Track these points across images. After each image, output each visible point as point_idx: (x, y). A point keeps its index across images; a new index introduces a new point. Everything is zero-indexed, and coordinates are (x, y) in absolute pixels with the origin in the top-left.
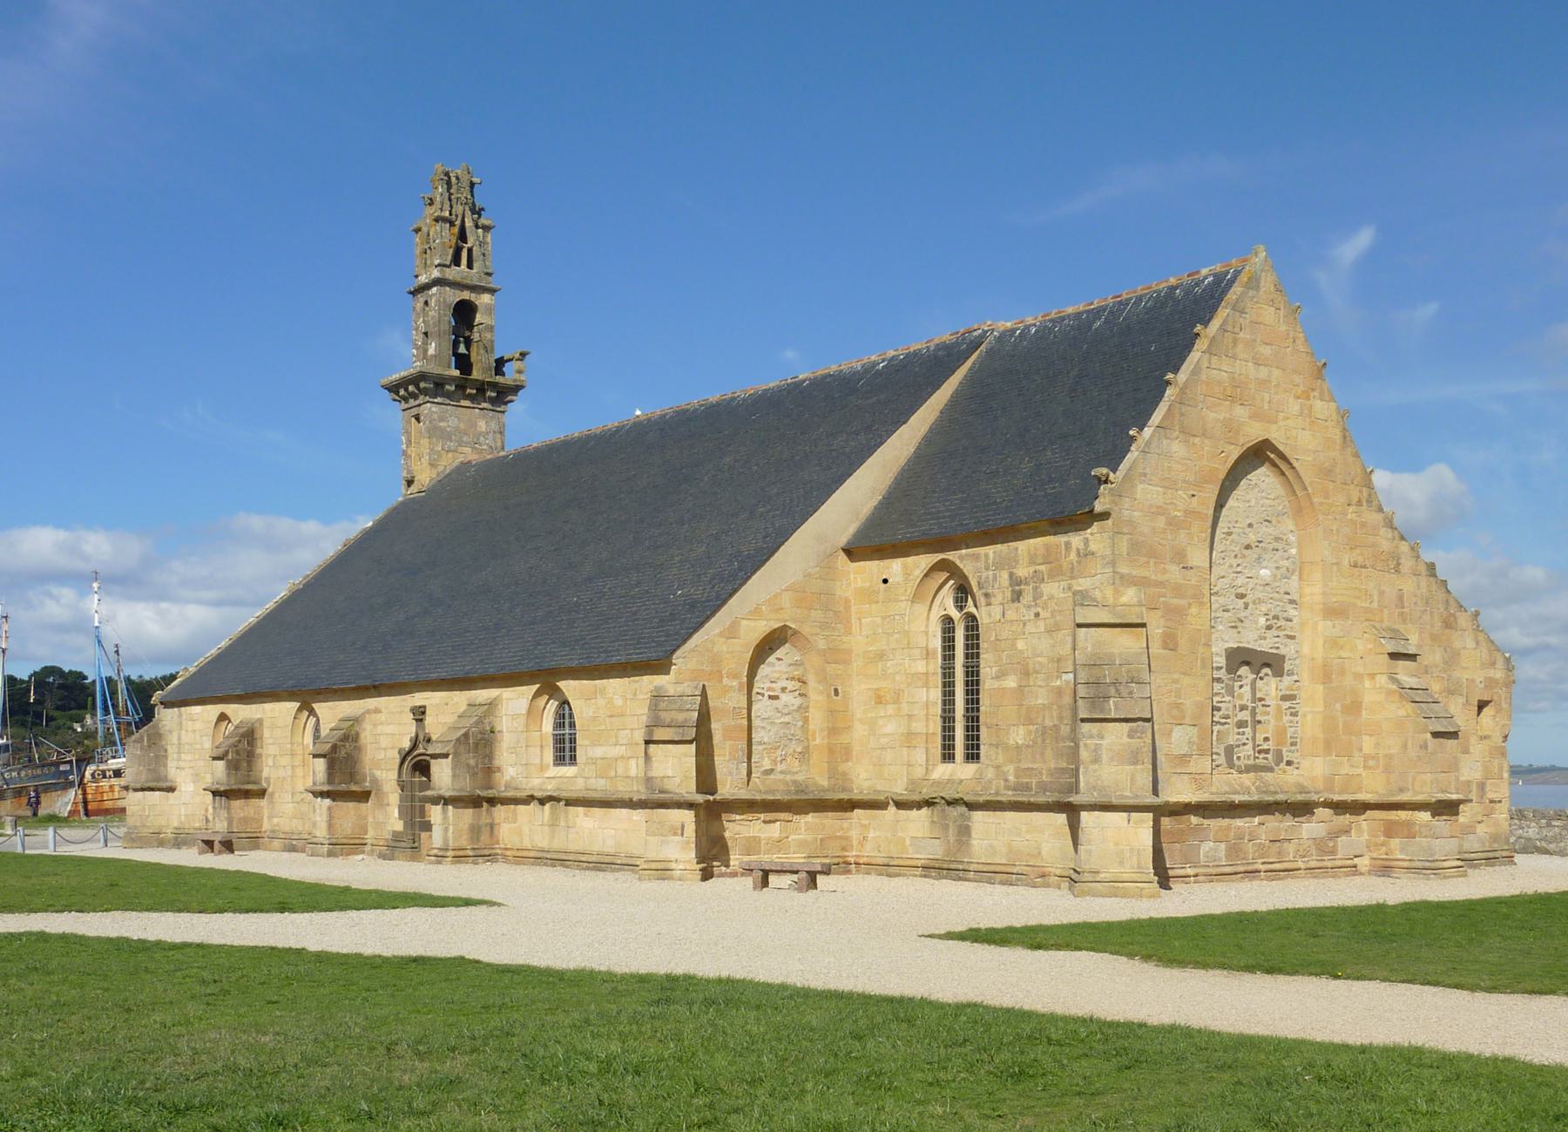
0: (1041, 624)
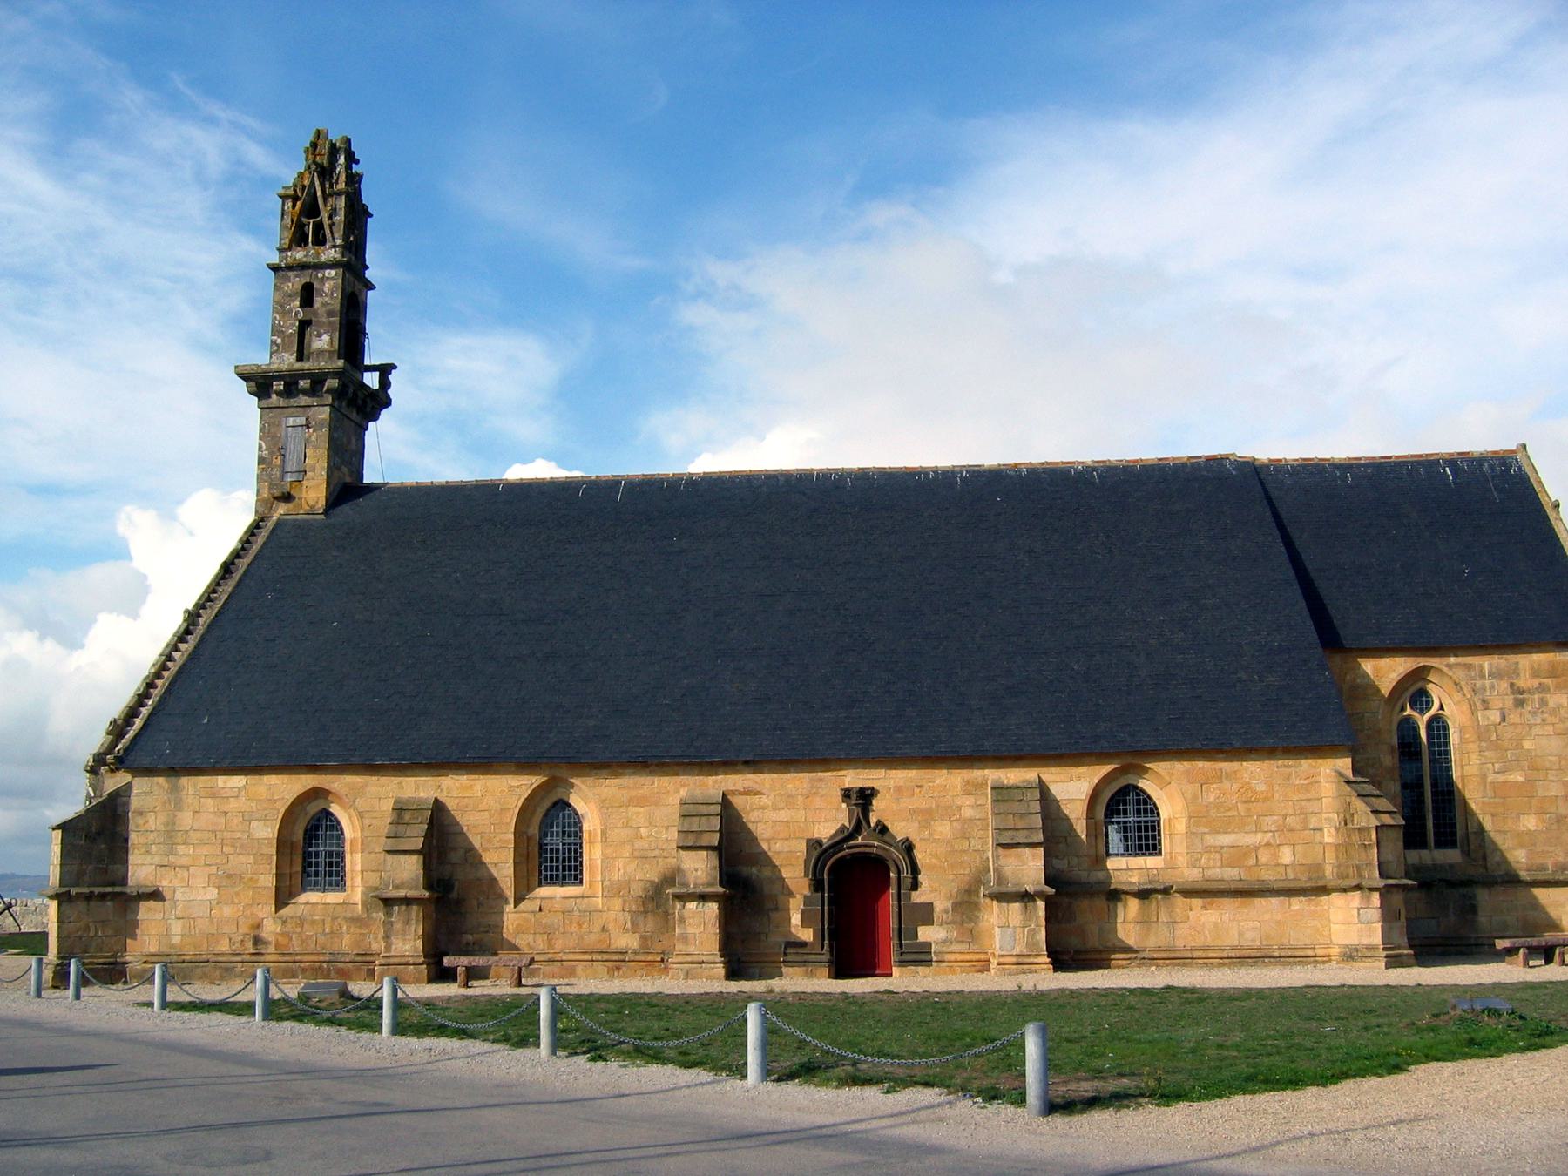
0: (1549, 730)
